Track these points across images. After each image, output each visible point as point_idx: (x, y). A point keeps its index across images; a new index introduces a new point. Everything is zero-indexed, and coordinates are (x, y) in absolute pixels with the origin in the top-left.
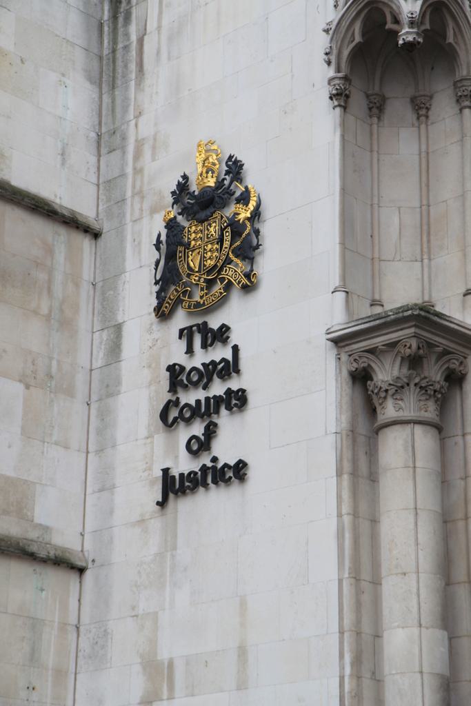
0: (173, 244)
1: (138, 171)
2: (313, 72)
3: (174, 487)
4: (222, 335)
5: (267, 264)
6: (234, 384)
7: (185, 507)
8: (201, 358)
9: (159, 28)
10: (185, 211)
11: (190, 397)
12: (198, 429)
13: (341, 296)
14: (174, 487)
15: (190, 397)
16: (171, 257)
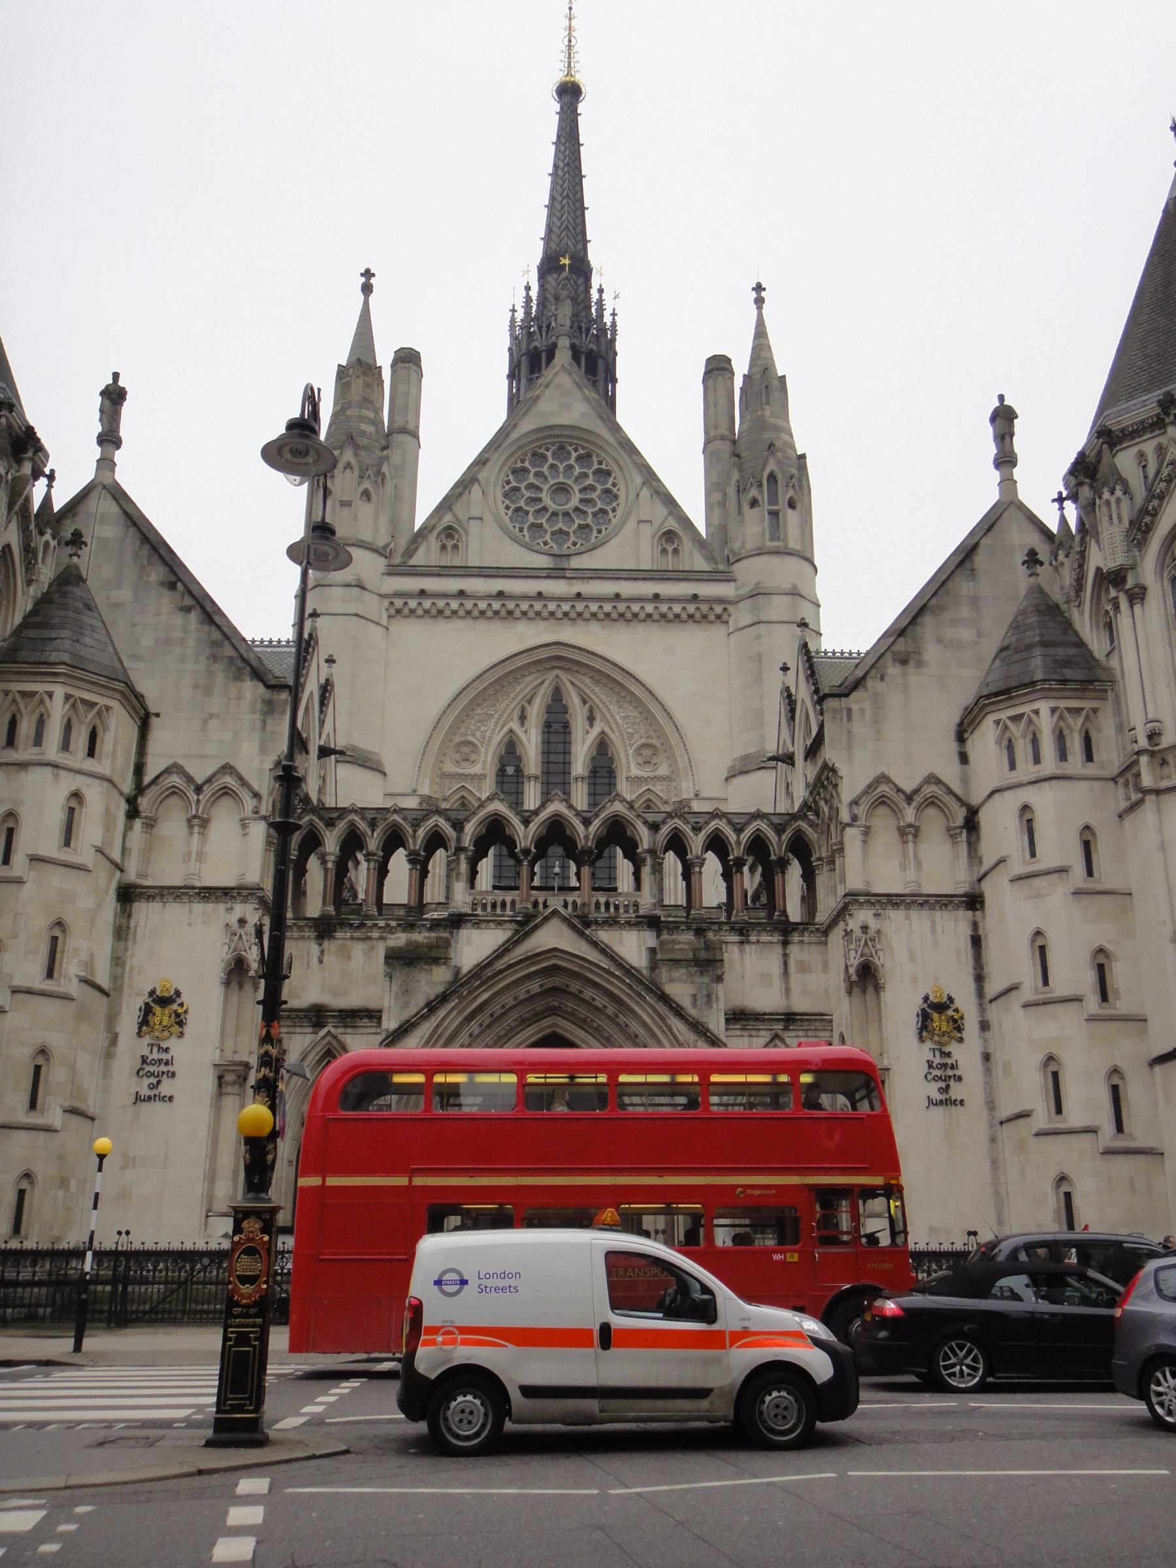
0: (147, 1011)
1: (131, 978)
2: (216, 973)
3: (139, 1099)
4: (167, 1050)
5: (187, 1030)
6: (169, 1068)
7: (145, 1106)
8: (156, 1055)
9: (145, 926)
10: (154, 1001)
11: (152, 1069)
12: (154, 1080)
13: (218, 1051)
14: (139, 1099)
15: (152, 1069)
16: (146, 1015)
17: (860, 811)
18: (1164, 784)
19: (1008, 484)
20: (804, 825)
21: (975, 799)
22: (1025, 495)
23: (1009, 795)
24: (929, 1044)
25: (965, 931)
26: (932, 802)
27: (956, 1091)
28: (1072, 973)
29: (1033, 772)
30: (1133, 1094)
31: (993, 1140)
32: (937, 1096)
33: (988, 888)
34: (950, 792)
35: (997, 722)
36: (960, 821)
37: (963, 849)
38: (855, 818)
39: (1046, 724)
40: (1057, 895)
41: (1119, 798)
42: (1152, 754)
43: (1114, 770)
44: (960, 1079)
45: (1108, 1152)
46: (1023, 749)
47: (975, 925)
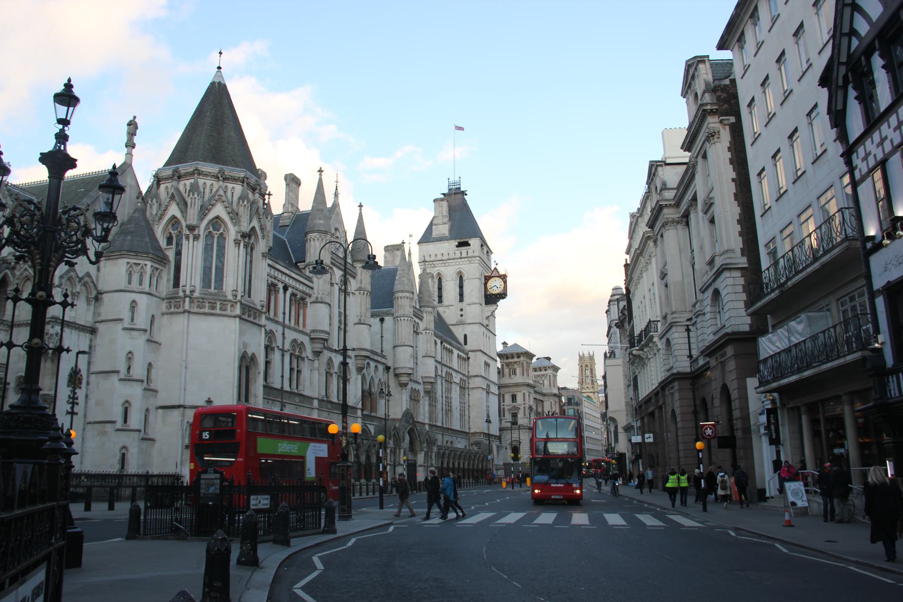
17: (64, 281)
18: (192, 310)
19: (129, 155)
20: (9, 272)
21: (101, 287)
22: (135, 165)
23: (127, 294)
24: (70, 389)
25: (88, 342)
26: (85, 284)
27: (76, 410)
28: (138, 371)
29: (139, 288)
30: (151, 418)
31: (84, 430)
32: (70, 410)
33: (101, 327)
34: (93, 282)
35: (128, 263)
36: (93, 296)
37: (92, 308)
38: (61, 285)
39: (148, 269)
40: (142, 339)
41: (164, 306)
42: (191, 298)
43: (164, 295)
44: (77, 404)
45: (143, 439)
46: (135, 277)
47: (91, 341)
